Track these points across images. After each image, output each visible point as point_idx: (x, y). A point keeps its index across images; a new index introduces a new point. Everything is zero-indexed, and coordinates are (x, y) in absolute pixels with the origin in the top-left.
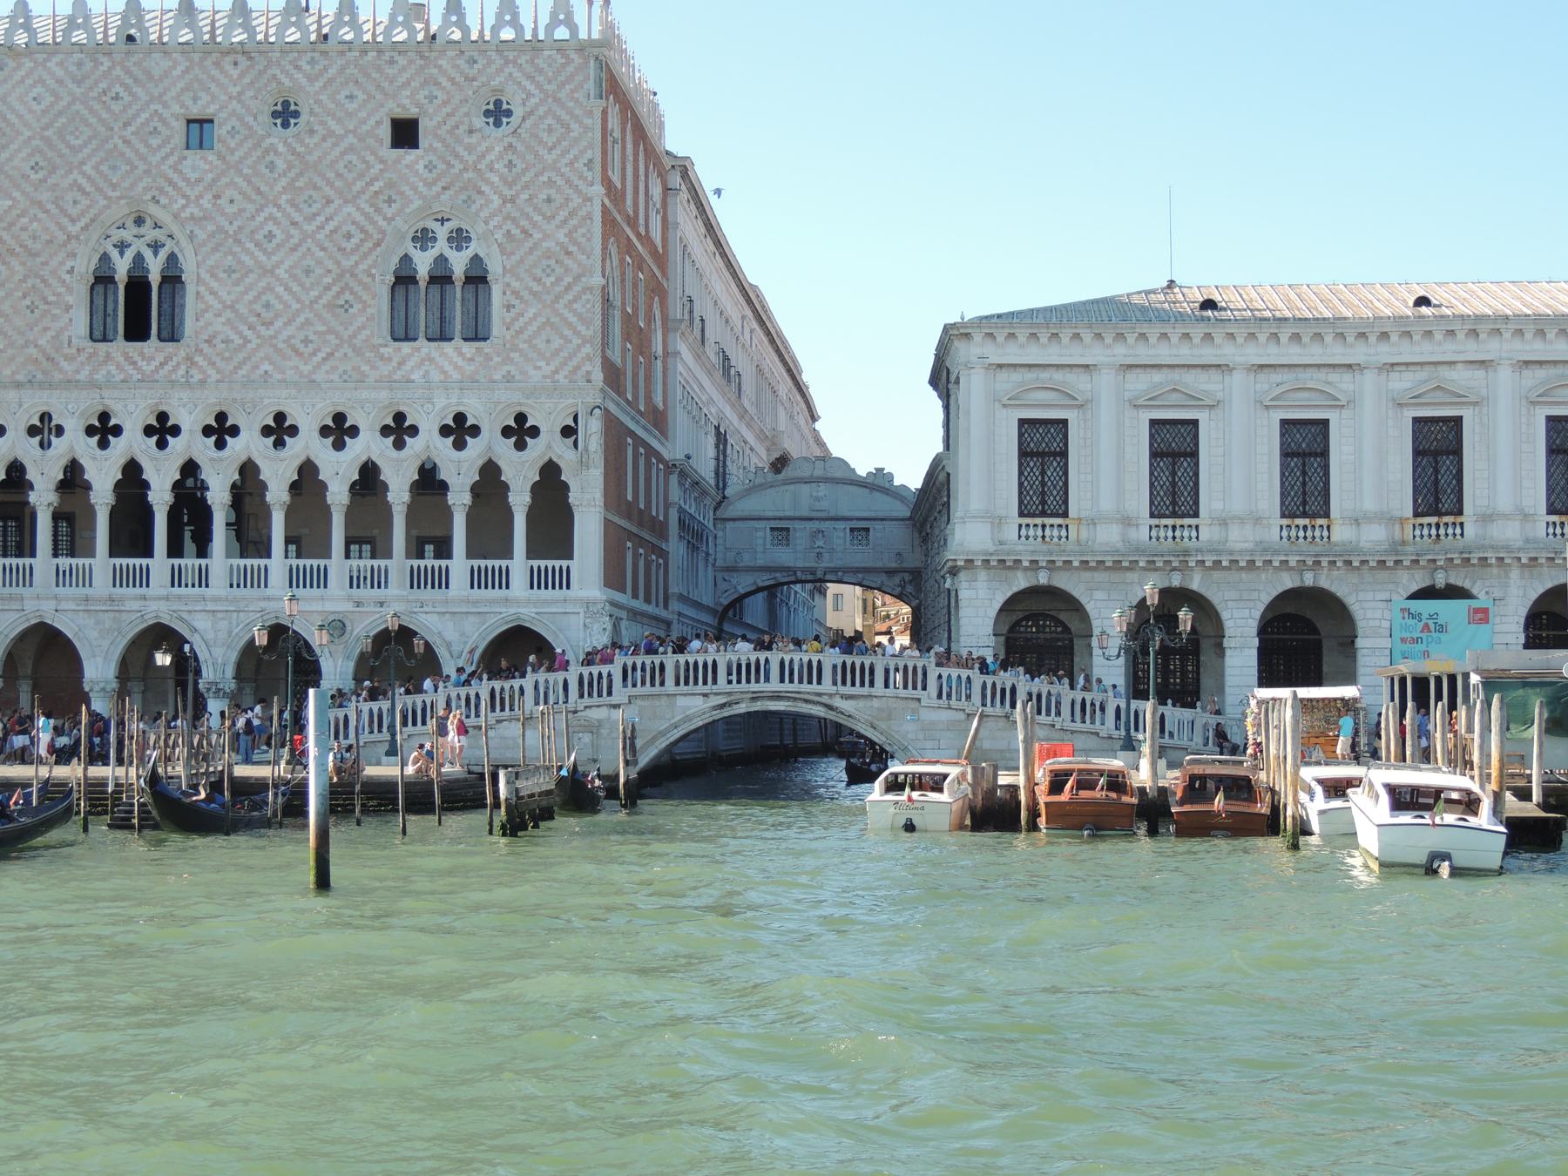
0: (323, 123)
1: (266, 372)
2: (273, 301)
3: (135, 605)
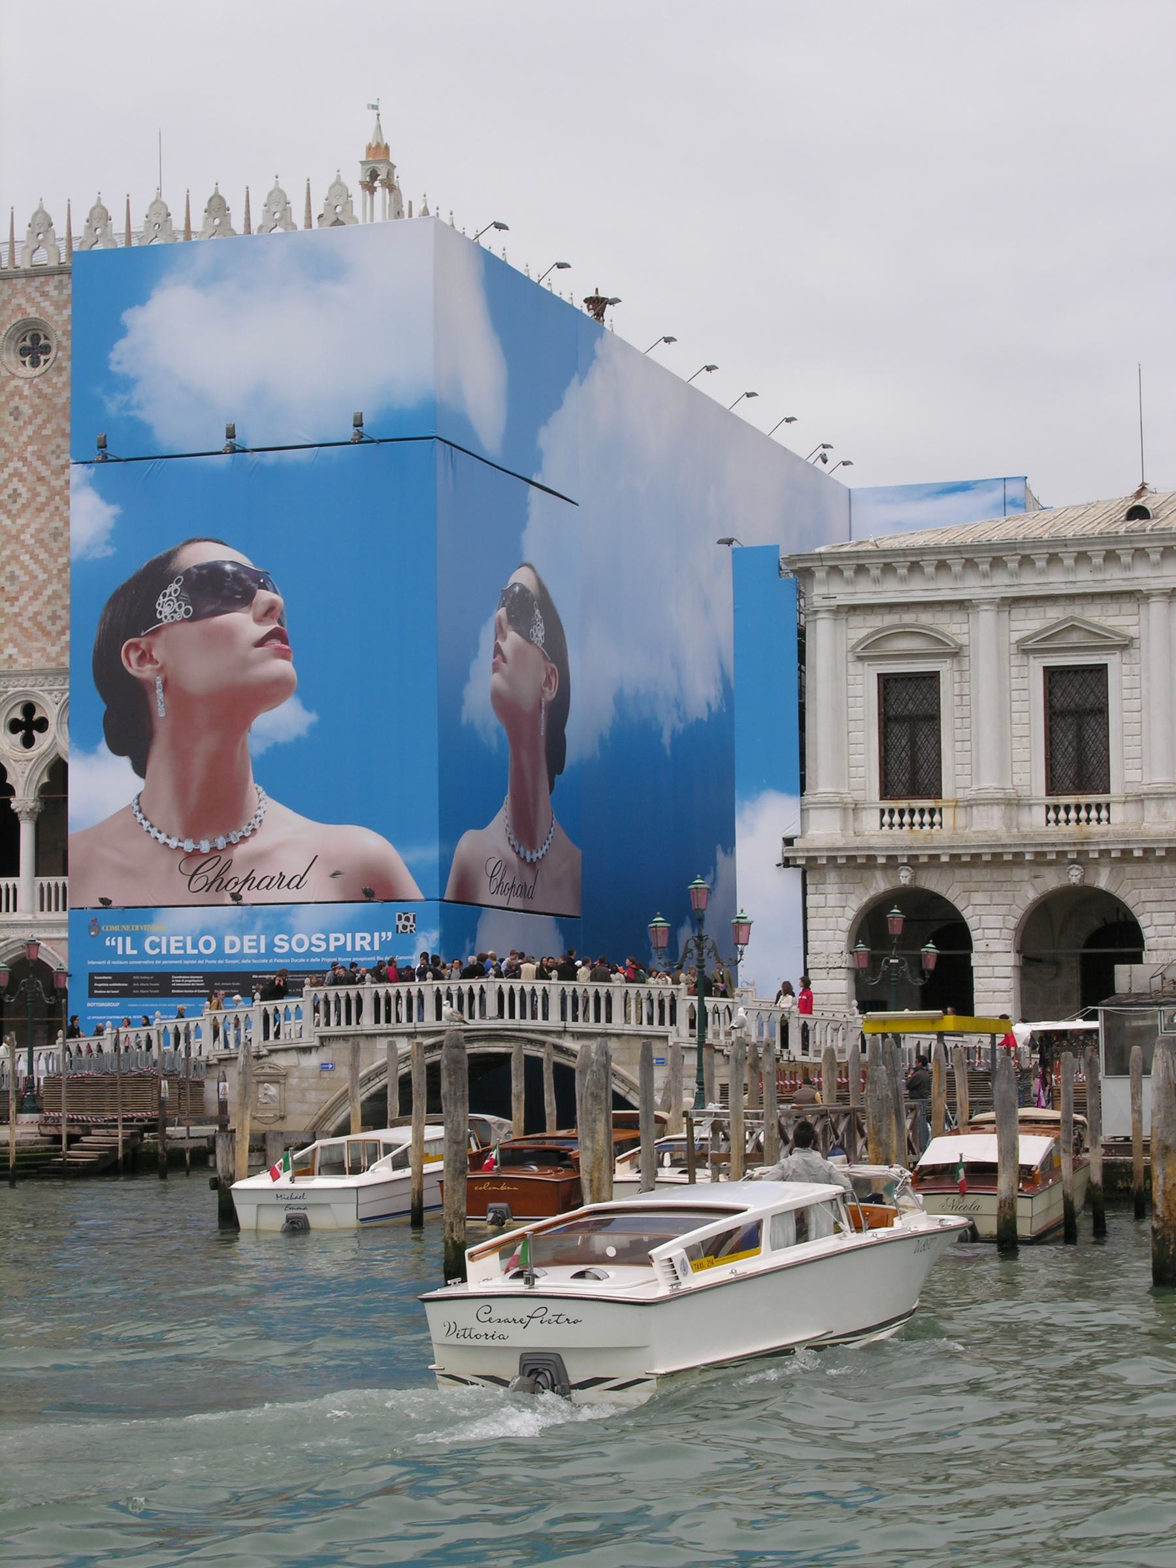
1: (10, 656)
2: (18, 572)
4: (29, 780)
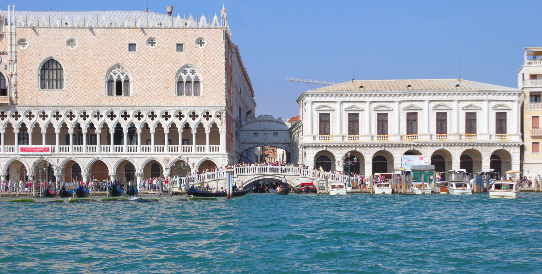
0: (161, 45)
2: (151, 87)
4: (154, 127)
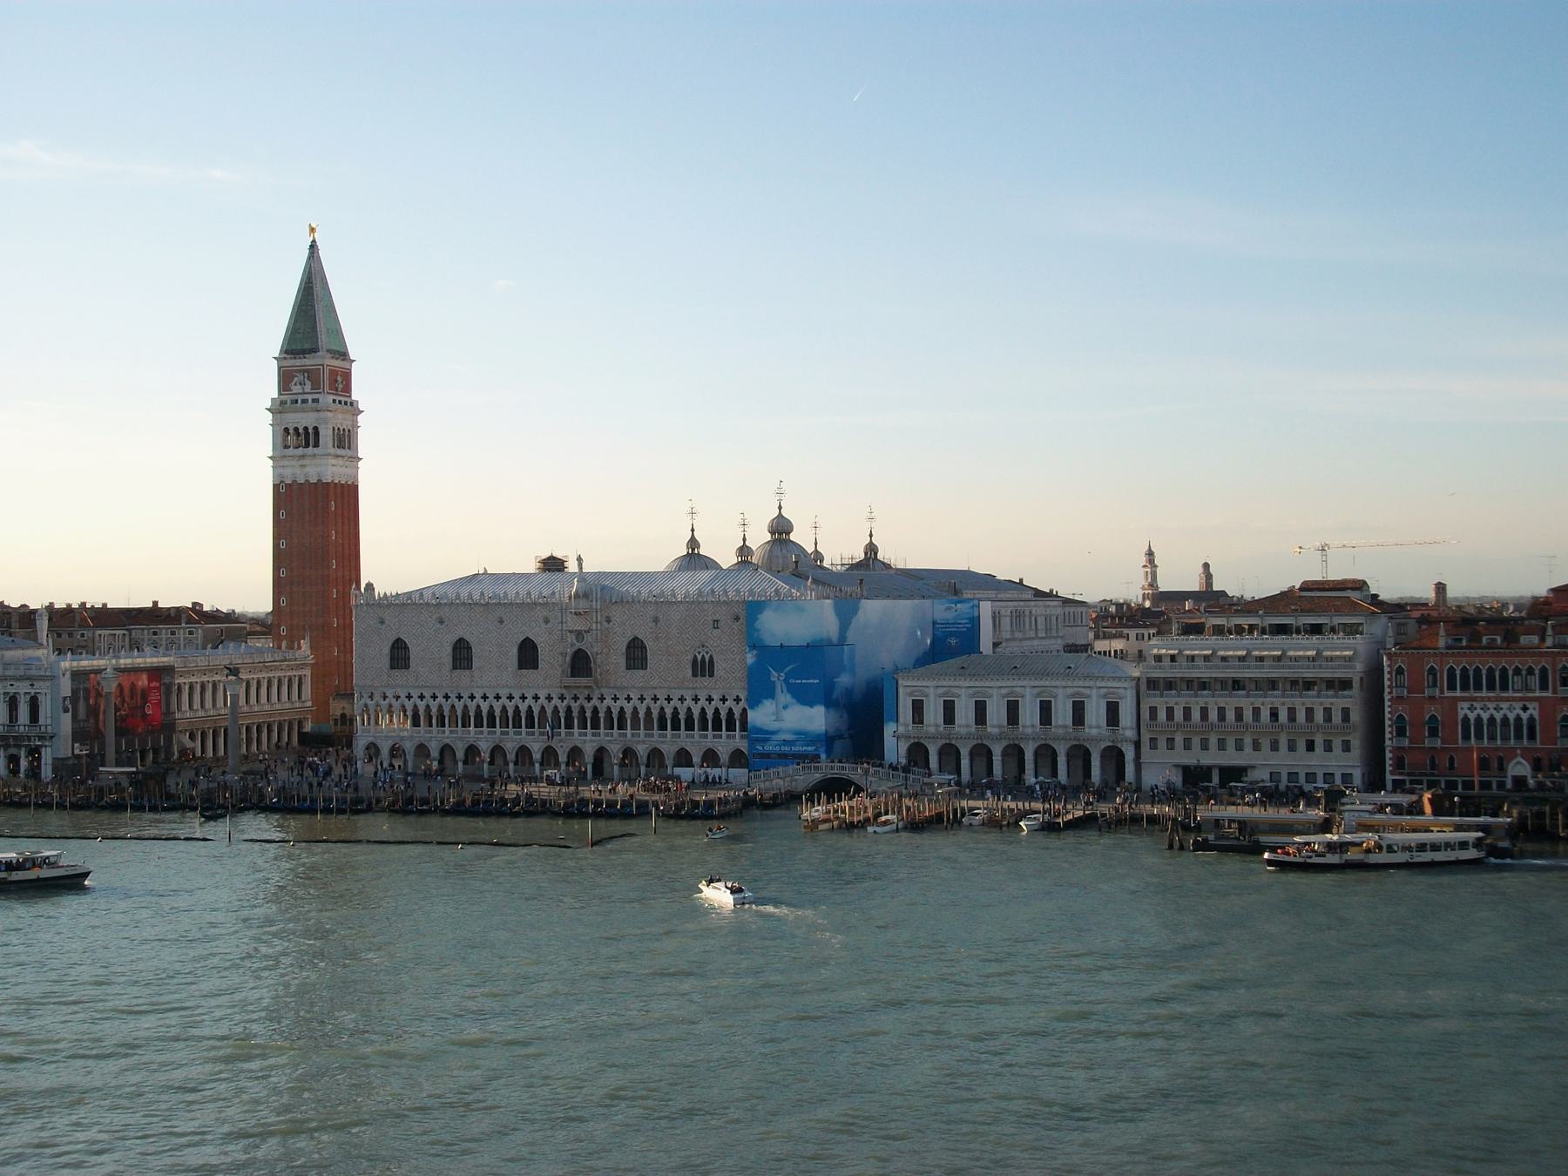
3: (704, 744)
